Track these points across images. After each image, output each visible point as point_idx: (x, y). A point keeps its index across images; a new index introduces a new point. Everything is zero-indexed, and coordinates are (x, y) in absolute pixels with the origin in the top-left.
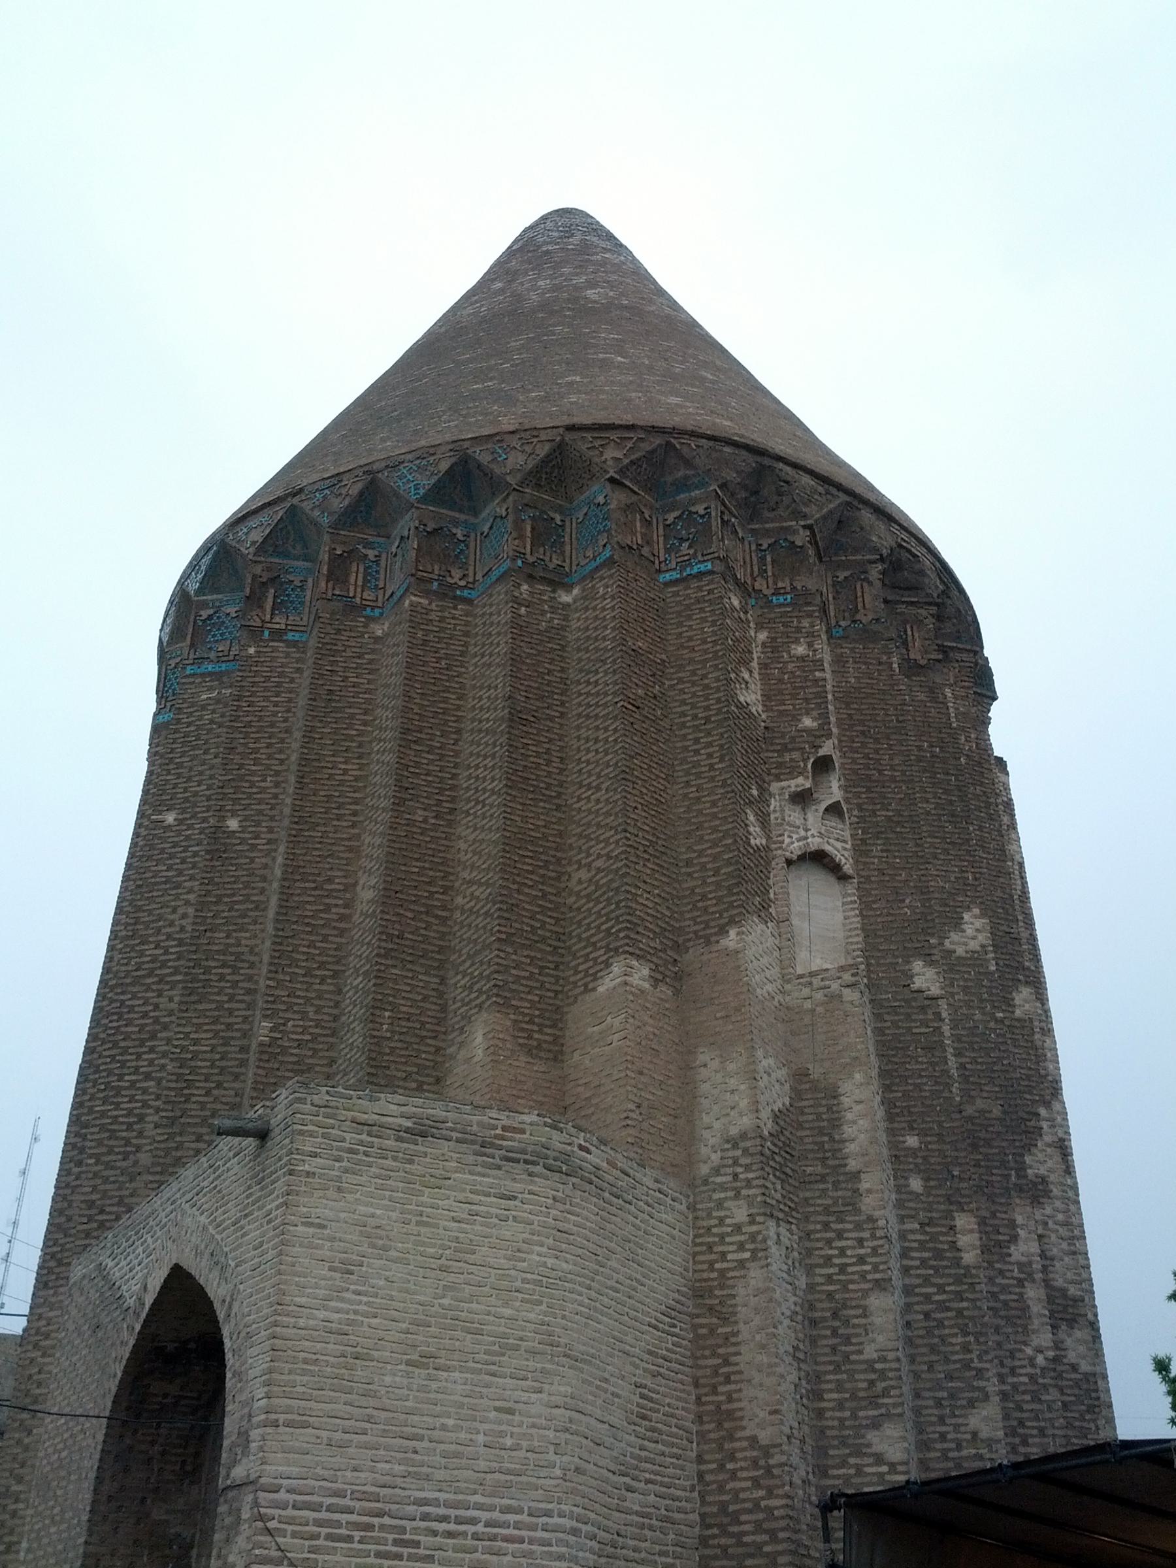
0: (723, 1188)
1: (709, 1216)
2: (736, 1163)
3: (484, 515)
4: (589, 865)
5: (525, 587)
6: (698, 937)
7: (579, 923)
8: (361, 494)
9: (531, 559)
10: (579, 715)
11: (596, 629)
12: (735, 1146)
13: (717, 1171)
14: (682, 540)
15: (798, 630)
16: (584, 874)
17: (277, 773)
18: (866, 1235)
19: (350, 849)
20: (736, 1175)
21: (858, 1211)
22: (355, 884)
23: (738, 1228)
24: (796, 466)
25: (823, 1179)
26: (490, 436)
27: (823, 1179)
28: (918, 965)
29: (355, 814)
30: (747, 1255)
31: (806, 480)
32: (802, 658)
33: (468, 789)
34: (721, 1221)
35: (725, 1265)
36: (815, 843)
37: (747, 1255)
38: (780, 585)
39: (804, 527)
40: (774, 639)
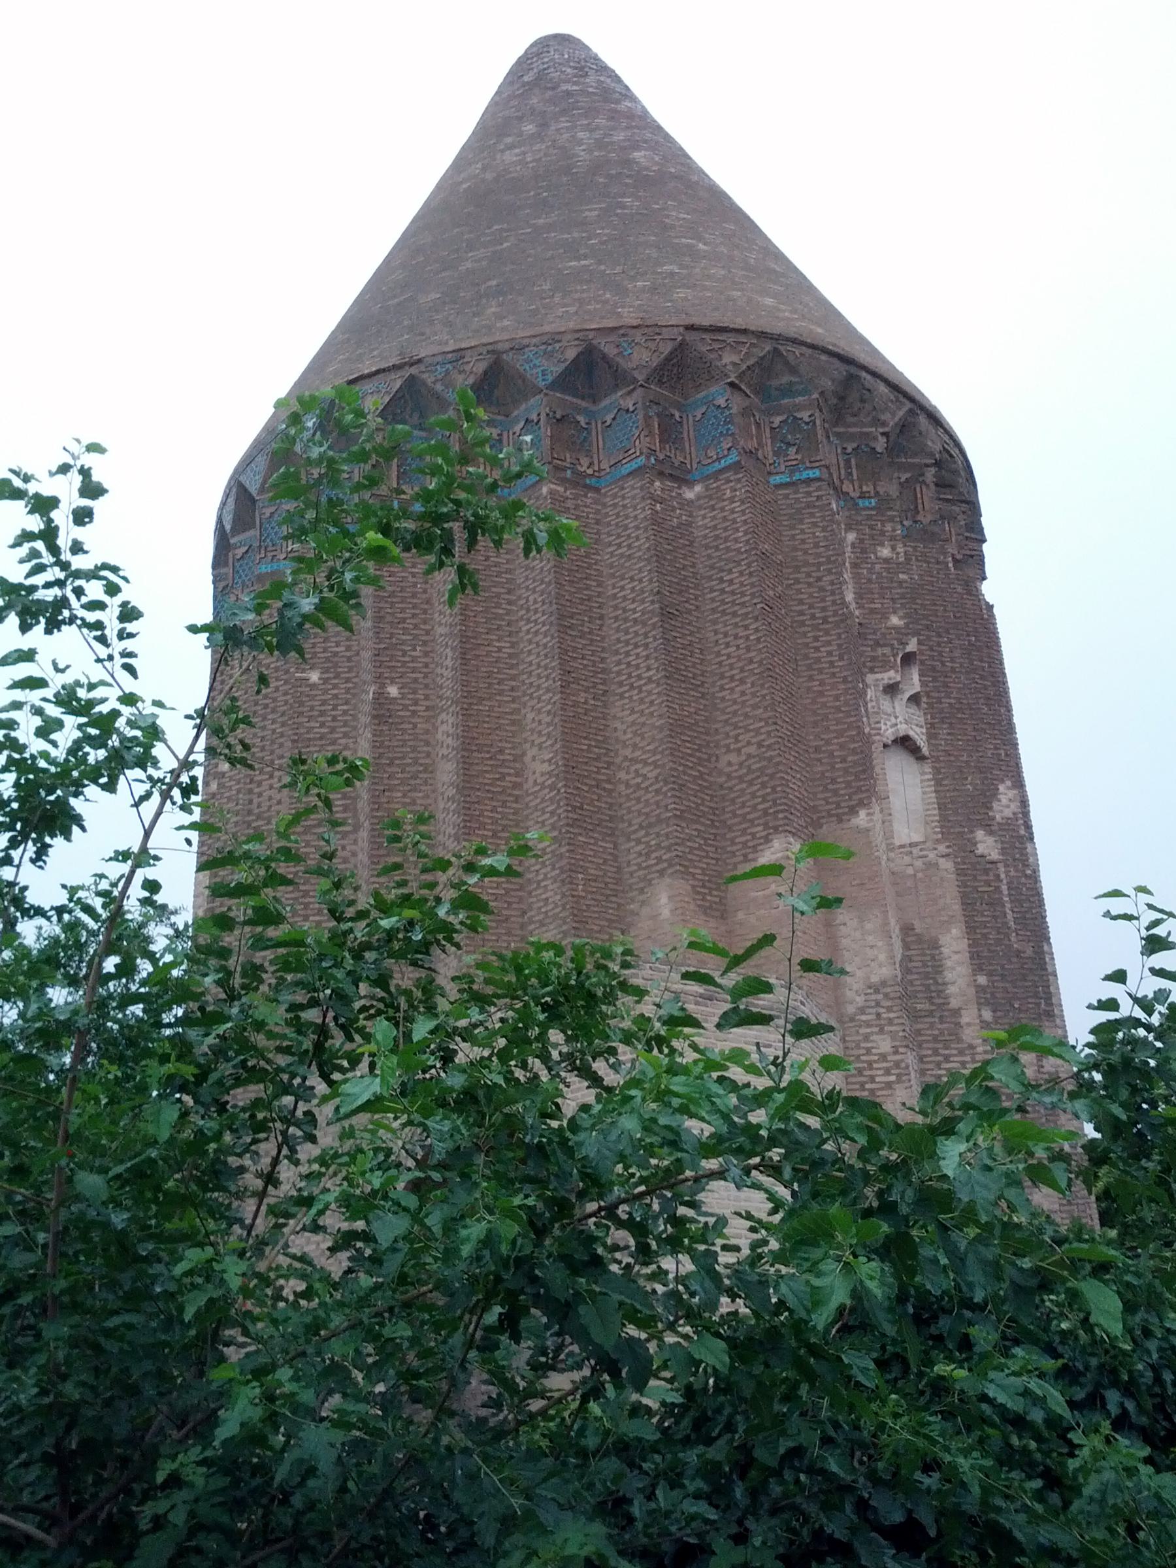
0: (868, 1024)
1: (858, 1047)
2: (878, 1004)
3: (606, 402)
4: (739, 750)
5: (657, 484)
6: (831, 816)
7: (733, 801)
8: (486, 373)
9: (661, 457)
10: (714, 610)
11: (725, 529)
12: (877, 991)
13: (862, 1011)
14: (789, 444)
15: (883, 533)
16: (732, 757)
17: (425, 643)
18: (968, 1059)
19: (513, 723)
20: (878, 1015)
21: (960, 1040)
22: (524, 754)
23: (883, 1057)
24: (875, 374)
25: (931, 1014)
26: (615, 328)
27: (931, 1014)
28: (980, 834)
29: (512, 689)
30: (893, 1078)
31: (882, 388)
32: (887, 561)
33: (619, 673)
34: (869, 1051)
35: (873, 1086)
36: (903, 729)
37: (893, 1078)
38: (865, 489)
39: (883, 434)
40: (862, 541)
